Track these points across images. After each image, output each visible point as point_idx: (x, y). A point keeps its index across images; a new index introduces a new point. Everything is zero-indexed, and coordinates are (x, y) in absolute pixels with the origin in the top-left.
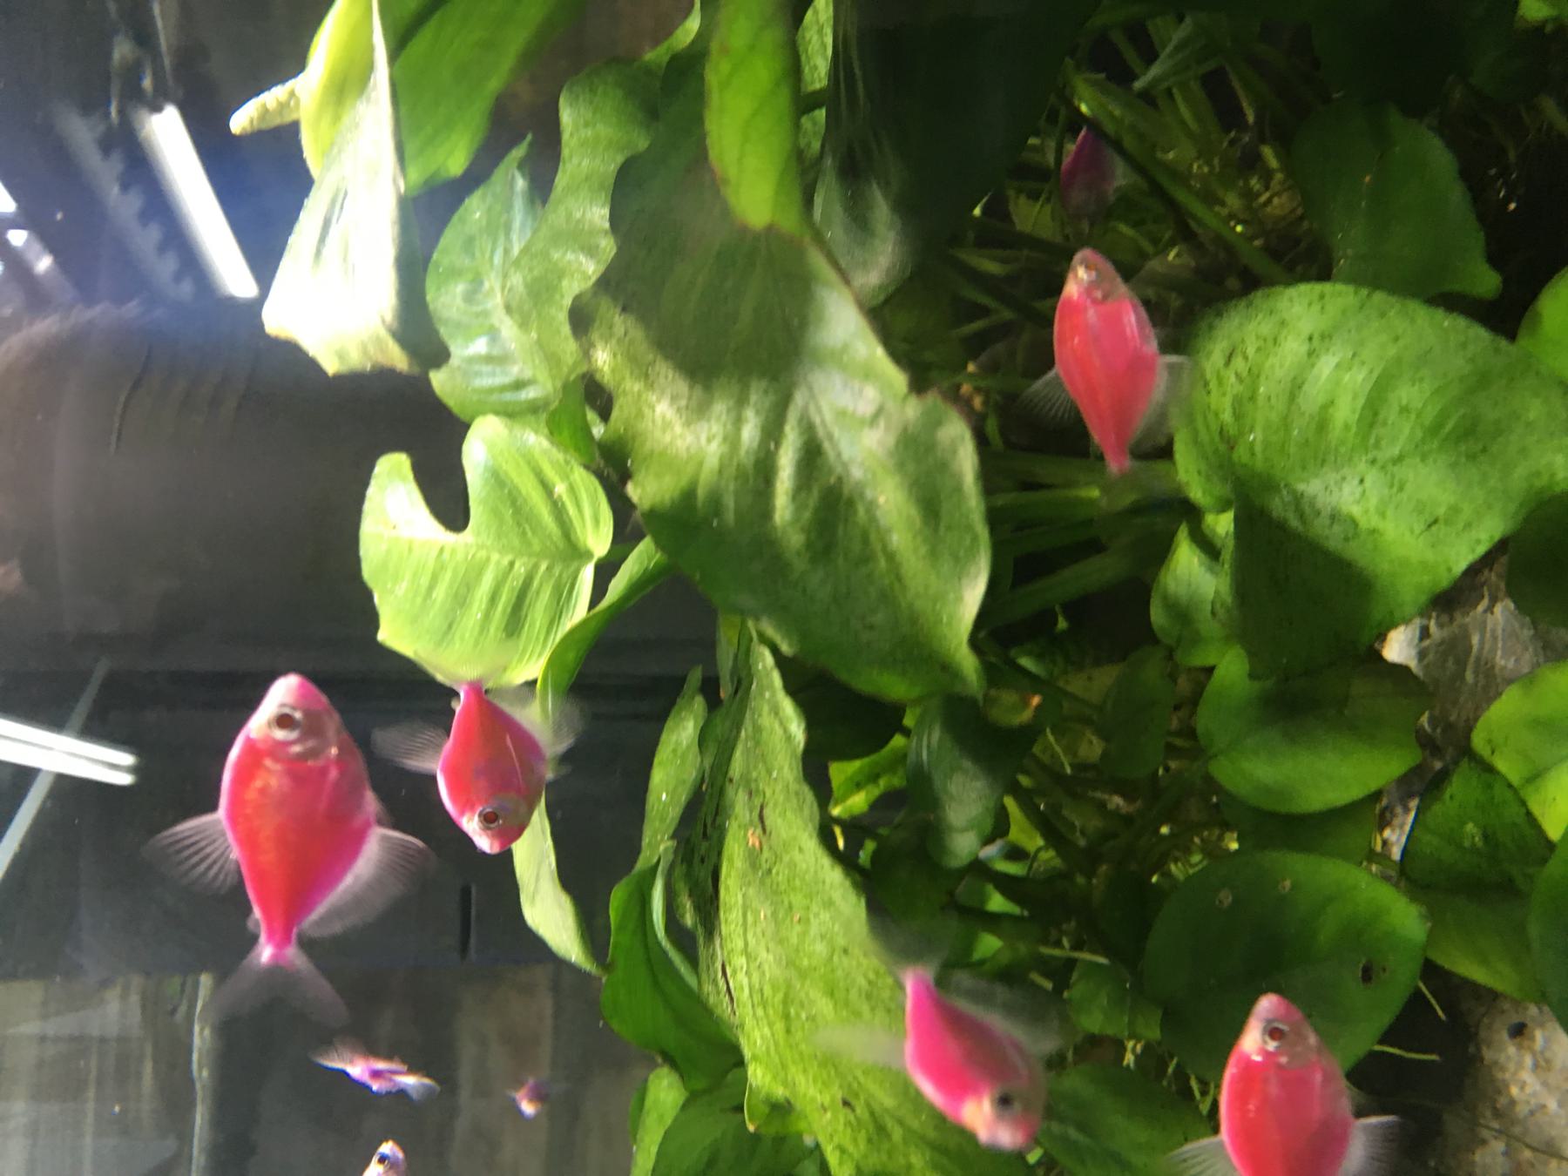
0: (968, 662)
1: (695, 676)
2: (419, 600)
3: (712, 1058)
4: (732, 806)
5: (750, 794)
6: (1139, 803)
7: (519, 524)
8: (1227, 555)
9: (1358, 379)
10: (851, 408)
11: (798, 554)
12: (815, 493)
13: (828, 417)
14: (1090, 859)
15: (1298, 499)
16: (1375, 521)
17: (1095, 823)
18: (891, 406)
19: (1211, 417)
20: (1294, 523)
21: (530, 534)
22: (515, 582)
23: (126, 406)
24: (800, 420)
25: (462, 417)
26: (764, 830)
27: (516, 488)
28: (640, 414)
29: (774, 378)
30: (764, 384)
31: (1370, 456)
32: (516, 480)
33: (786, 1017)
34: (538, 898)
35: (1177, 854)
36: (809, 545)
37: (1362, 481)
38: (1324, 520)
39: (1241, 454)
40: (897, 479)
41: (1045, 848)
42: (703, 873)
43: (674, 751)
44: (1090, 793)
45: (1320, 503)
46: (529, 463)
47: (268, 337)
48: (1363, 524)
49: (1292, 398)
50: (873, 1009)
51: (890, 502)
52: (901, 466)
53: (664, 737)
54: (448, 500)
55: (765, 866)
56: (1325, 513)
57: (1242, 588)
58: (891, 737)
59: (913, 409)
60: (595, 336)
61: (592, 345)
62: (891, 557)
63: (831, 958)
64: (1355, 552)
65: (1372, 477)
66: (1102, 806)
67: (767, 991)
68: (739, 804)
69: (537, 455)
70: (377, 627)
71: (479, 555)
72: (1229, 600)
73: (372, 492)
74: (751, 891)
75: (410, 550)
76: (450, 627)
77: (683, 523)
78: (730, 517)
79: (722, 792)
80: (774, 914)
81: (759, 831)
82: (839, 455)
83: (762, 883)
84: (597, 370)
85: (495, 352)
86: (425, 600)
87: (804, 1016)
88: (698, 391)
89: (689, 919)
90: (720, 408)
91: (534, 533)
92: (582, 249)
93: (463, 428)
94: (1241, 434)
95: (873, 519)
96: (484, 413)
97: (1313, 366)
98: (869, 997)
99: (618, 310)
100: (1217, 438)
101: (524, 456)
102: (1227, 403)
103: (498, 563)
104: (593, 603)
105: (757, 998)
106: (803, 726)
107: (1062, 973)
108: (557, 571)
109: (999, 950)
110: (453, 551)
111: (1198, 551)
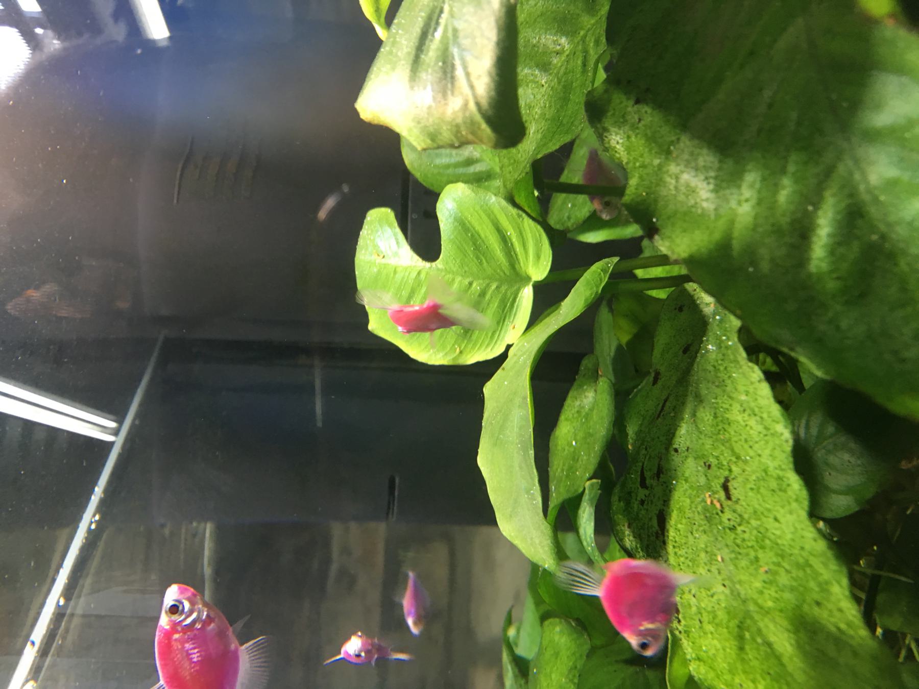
7: (478, 258)
12: (856, 246)
23: (181, 175)
26: (728, 497)
28: (660, 182)
32: (478, 228)
43: (578, 412)
46: (489, 216)
47: (362, 120)
60: (607, 122)
61: (606, 130)
69: (497, 210)
70: (367, 322)
73: (364, 233)
75: (395, 272)
78: (765, 266)
81: (722, 495)
88: (729, 164)
90: (752, 177)
92: (537, 66)
99: (631, 102)
101: (485, 211)
103: (460, 282)
108: (503, 289)
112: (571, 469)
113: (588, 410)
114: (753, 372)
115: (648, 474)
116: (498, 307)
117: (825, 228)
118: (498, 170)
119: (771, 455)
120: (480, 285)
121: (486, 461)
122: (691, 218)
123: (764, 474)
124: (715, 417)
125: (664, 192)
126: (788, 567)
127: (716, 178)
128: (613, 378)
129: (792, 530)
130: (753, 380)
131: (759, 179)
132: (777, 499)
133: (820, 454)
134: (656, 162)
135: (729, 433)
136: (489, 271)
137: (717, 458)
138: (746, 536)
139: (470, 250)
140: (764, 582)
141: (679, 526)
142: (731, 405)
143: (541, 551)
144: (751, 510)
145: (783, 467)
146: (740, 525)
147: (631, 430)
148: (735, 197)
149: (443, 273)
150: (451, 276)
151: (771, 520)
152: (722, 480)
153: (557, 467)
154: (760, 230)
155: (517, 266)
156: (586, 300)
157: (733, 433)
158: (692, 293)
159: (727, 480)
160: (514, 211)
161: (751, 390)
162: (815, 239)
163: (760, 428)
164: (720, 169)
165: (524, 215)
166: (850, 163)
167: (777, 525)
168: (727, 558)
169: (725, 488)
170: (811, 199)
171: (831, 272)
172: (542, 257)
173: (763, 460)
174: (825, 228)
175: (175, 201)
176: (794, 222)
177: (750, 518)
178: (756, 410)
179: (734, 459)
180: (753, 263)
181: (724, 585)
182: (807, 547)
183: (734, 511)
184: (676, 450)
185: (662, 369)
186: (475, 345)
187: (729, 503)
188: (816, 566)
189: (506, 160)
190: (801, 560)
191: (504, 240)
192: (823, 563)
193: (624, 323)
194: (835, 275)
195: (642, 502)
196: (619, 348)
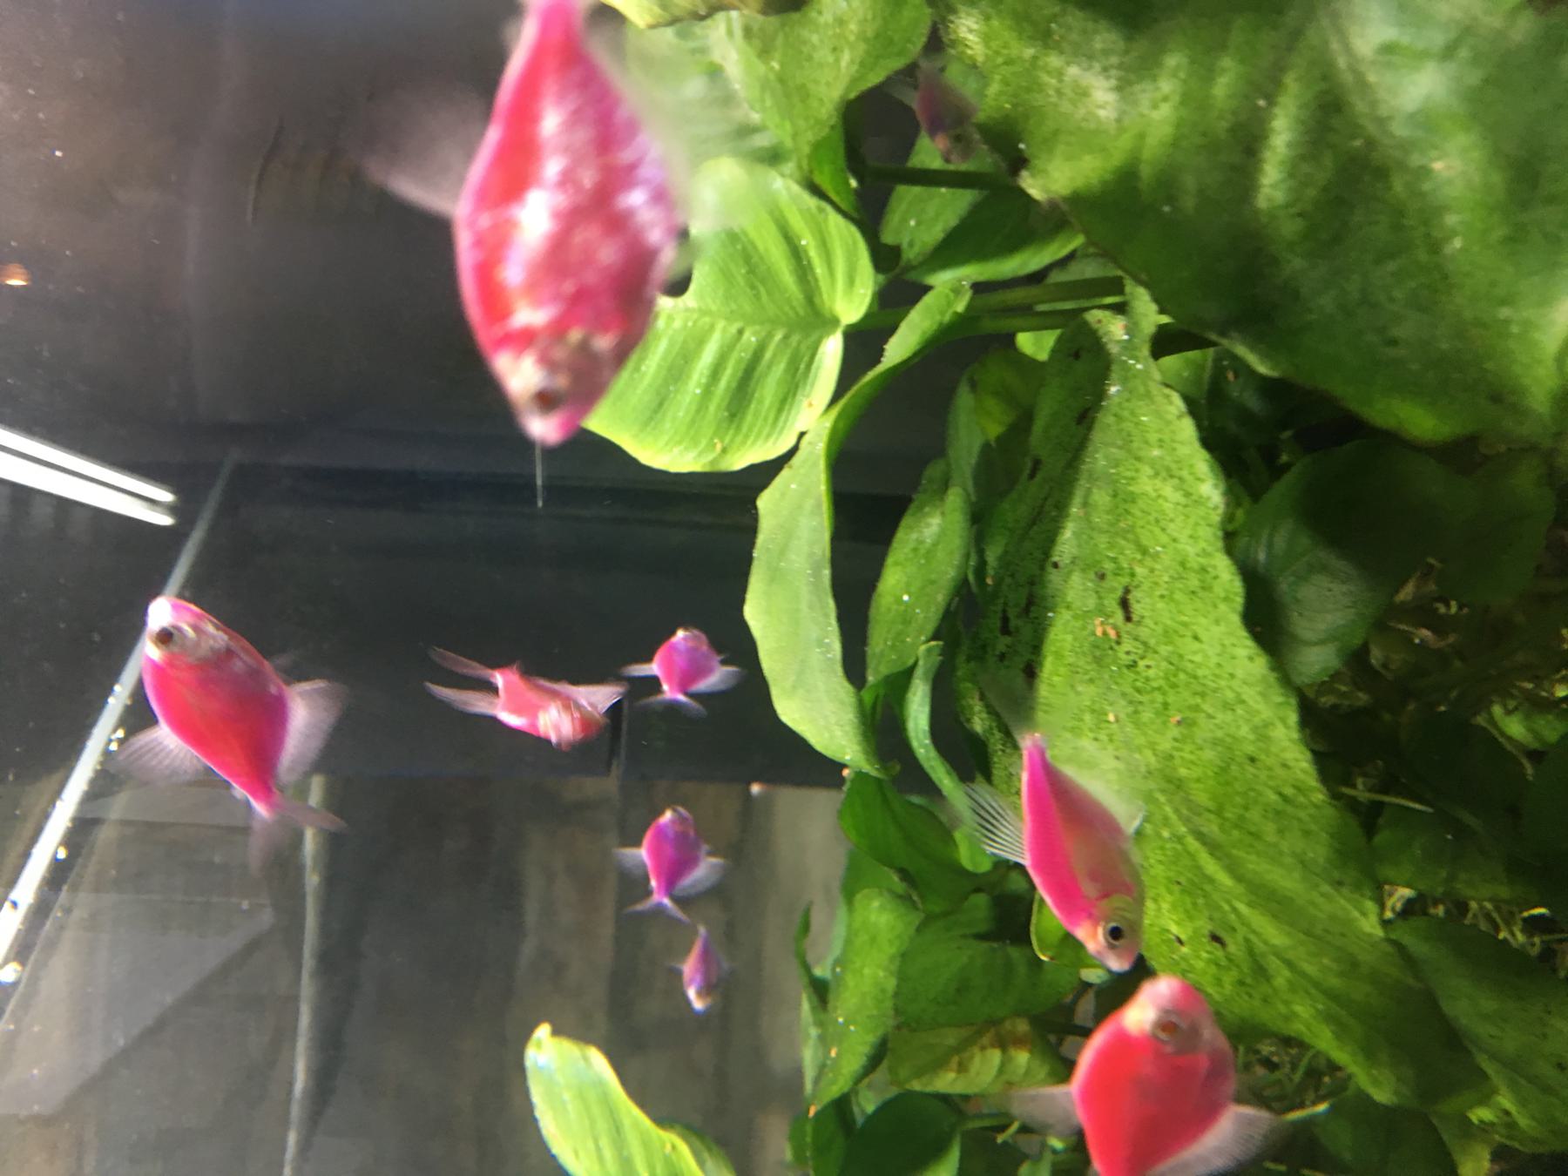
7: (753, 287)
12: (1328, 160)
17: (1398, 659)
21: (764, 298)
22: (741, 354)
26: (1128, 619)
32: (753, 234)
43: (915, 550)
46: (771, 213)
50: (1281, 832)
51: (1454, 169)
55: (1126, 659)
66: (1407, 639)
69: (784, 198)
71: (700, 323)
76: (661, 404)
78: (1189, 203)
81: (1119, 615)
82: (1374, 104)
91: (769, 293)
103: (724, 330)
106: (1222, 486)
108: (795, 339)
112: (899, 637)
113: (927, 553)
114: (1171, 403)
115: (1012, 613)
116: (787, 370)
117: (1283, 133)
118: (789, 143)
119: (1191, 537)
123: (1180, 569)
124: (1115, 496)
125: (1038, 100)
126: (1210, 711)
128: (971, 488)
129: (1218, 649)
130: (1170, 417)
132: (1199, 604)
133: (1284, 585)
135: (1133, 515)
137: (1114, 560)
138: (1151, 673)
139: (740, 272)
140: (1176, 740)
141: (1056, 679)
142: (1137, 471)
143: (838, 733)
144: (1159, 629)
145: (1210, 549)
146: (1142, 658)
147: (992, 556)
149: (695, 316)
150: (707, 319)
151: (1189, 640)
152: (1119, 593)
153: (879, 642)
155: (817, 300)
157: (1138, 513)
158: (1096, 326)
159: (1127, 591)
160: (812, 202)
161: (1166, 437)
162: (1267, 155)
163: (1177, 497)
165: (829, 208)
167: (1196, 645)
168: (1122, 716)
169: (1125, 604)
171: (1287, 206)
172: (858, 282)
173: (1180, 546)
174: (1283, 133)
175: (249, 217)
176: (1233, 130)
177: (1158, 643)
178: (1173, 466)
179: (1139, 557)
180: (1171, 199)
181: (1117, 758)
182: (1240, 673)
183: (1136, 639)
184: (1056, 565)
186: (747, 437)
187: (1130, 625)
188: (1251, 703)
189: (801, 123)
190: (1230, 695)
192: (1261, 694)
193: (991, 403)
194: (1293, 211)
195: (1002, 657)
196: (986, 447)
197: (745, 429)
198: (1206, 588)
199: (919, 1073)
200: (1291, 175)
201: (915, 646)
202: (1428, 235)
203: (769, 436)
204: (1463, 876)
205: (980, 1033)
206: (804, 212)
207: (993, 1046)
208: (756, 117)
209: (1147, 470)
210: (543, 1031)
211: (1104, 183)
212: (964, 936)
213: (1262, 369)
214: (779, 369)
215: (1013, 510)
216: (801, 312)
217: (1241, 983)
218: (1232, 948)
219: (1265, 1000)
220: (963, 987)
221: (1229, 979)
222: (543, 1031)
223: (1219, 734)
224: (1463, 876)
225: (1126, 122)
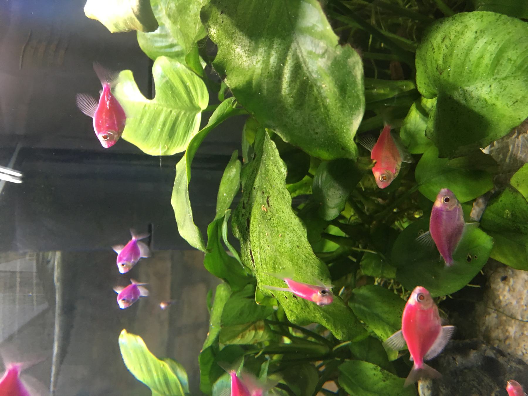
0: (352, 146)
1: (235, 154)
2: (137, 124)
3: (243, 281)
4: (255, 197)
5: (263, 193)
6: (387, 201)
7: (174, 97)
8: (432, 114)
9: (493, 48)
10: (314, 51)
11: (291, 105)
13: (305, 54)
14: (371, 218)
15: (465, 92)
16: (494, 101)
17: (372, 207)
18: (331, 49)
19: (434, 62)
20: (463, 102)
21: (178, 101)
24: (293, 55)
25: (151, 58)
26: (269, 206)
27: (173, 83)
29: (284, 39)
30: (279, 41)
31: (494, 77)
32: (173, 81)
33: (274, 268)
34: (184, 228)
35: (399, 218)
36: (295, 102)
37: (490, 86)
38: (474, 100)
39: (444, 75)
40: (331, 78)
41: (354, 215)
42: (243, 220)
43: (228, 179)
44: (371, 197)
45: (473, 94)
46: (177, 74)
48: (489, 102)
49: (467, 55)
51: (327, 87)
52: (332, 73)
53: (224, 174)
54: (148, 89)
55: (269, 218)
56: (475, 99)
57: (438, 125)
58: (304, 176)
59: (339, 51)
62: (326, 107)
63: (292, 249)
64: (484, 112)
65: (494, 85)
66: (373, 201)
67: (268, 259)
68: (258, 198)
72: (433, 130)
74: (262, 226)
76: (148, 134)
77: (247, 93)
79: (250, 193)
80: (271, 234)
81: (267, 206)
83: (267, 222)
84: (211, 36)
85: (163, 33)
86: (139, 124)
87: (281, 268)
89: (237, 235)
90: (261, 50)
93: (151, 62)
94: (445, 68)
95: (320, 93)
96: (161, 55)
97: (476, 42)
98: (305, 261)
100: (435, 70)
101: (175, 72)
102: (441, 56)
103: (166, 111)
104: (201, 128)
105: (263, 262)
106: (286, 169)
107: (359, 256)
109: (338, 249)
110: (149, 106)
111: (419, 113)
120: (176, 112)
121: (174, 202)
122: (239, 70)
127: (248, 50)
131: (263, 51)
134: (228, 43)
136: (180, 104)
144: (275, 209)
148: (255, 60)
149: (157, 106)
151: (281, 212)
154: (264, 75)
155: (193, 102)
156: (218, 117)
159: (268, 198)
160: (190, 72)
163: (277, 171)
164: (250, 46)
165: (194, 74)
166: (296, 46)
167: (283, 214)
169: (268, 201)
170: (282, 60)
171: (289, 94)
172: (204, 96)
176: (276, 71)
180: (260, 91)
184: (254, 188)
185: (257, 152)
191: (186, 87)
195: (243, 215)
197: (174, 141)
198: (284, 198)
199: (229, 339)
200: (290, 86)
201: (225, 210)
202: (323, 104)
203: (181, 145)
204: (385, 272)
205: (249, 326)
206: (187, 75)
207: (253, 329)
208: (175, 42)
209: (271, 163)
210: (124, 332)
211: (243, 85)
212: (244, 298)
213: (284, 140)
214: (184, 123)
215: (248, 170)
216: (189, 106)
217: (302, 308)
218: (299, 299)
219: (308, 313)
220: (241, 313)
221: (299, 307)
222: (124, 332)
223: (290, 239)
224: (385, 272)
225: (250, 67)
